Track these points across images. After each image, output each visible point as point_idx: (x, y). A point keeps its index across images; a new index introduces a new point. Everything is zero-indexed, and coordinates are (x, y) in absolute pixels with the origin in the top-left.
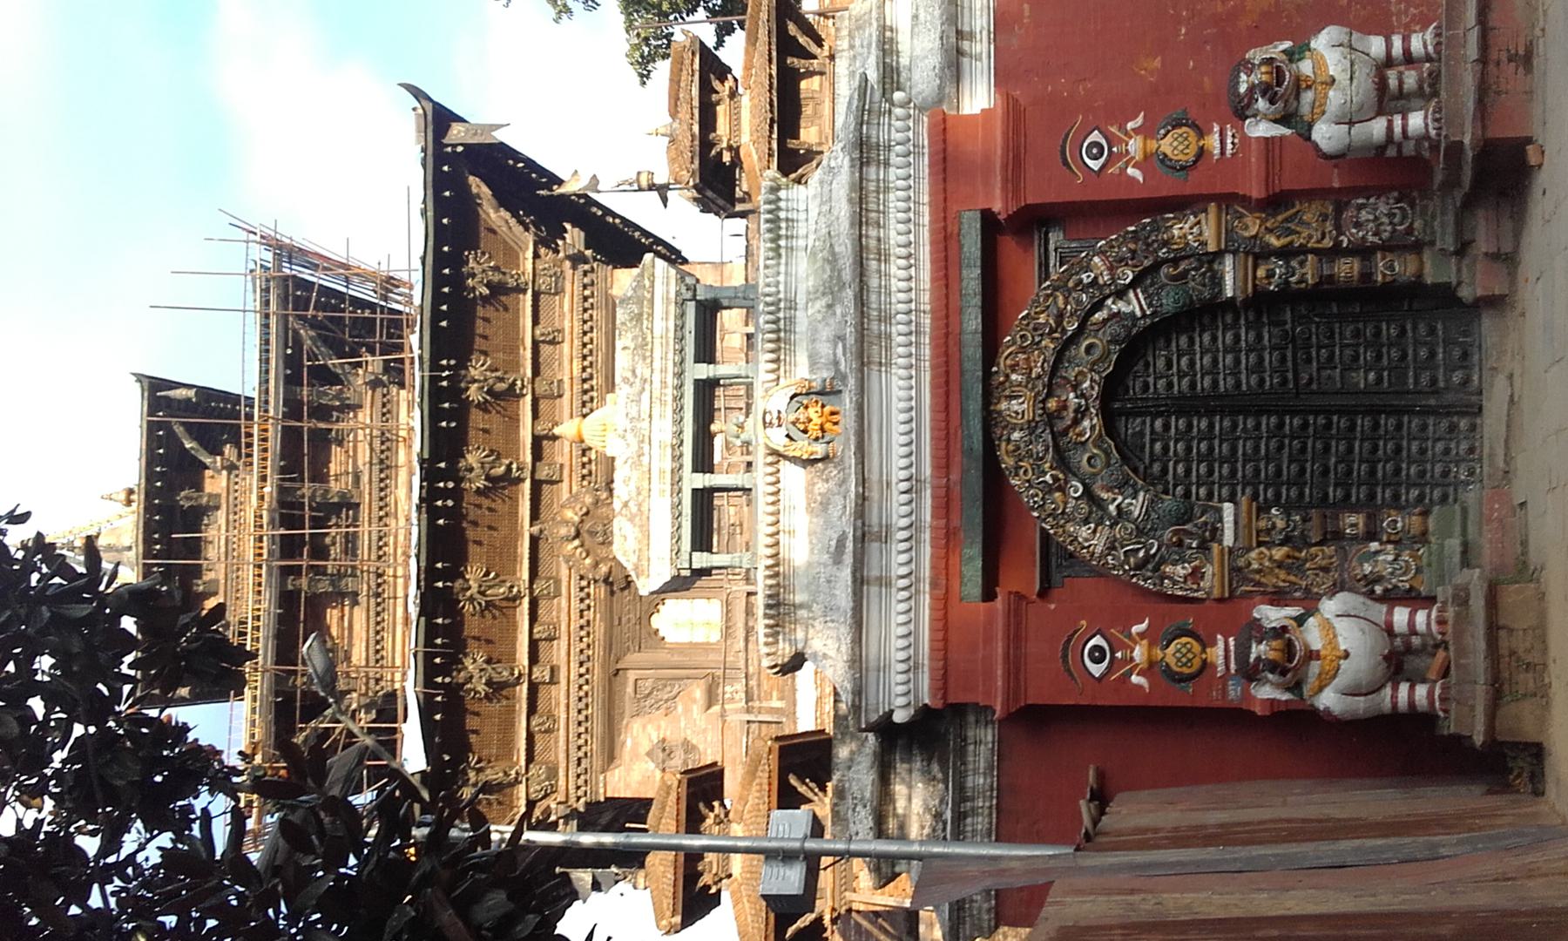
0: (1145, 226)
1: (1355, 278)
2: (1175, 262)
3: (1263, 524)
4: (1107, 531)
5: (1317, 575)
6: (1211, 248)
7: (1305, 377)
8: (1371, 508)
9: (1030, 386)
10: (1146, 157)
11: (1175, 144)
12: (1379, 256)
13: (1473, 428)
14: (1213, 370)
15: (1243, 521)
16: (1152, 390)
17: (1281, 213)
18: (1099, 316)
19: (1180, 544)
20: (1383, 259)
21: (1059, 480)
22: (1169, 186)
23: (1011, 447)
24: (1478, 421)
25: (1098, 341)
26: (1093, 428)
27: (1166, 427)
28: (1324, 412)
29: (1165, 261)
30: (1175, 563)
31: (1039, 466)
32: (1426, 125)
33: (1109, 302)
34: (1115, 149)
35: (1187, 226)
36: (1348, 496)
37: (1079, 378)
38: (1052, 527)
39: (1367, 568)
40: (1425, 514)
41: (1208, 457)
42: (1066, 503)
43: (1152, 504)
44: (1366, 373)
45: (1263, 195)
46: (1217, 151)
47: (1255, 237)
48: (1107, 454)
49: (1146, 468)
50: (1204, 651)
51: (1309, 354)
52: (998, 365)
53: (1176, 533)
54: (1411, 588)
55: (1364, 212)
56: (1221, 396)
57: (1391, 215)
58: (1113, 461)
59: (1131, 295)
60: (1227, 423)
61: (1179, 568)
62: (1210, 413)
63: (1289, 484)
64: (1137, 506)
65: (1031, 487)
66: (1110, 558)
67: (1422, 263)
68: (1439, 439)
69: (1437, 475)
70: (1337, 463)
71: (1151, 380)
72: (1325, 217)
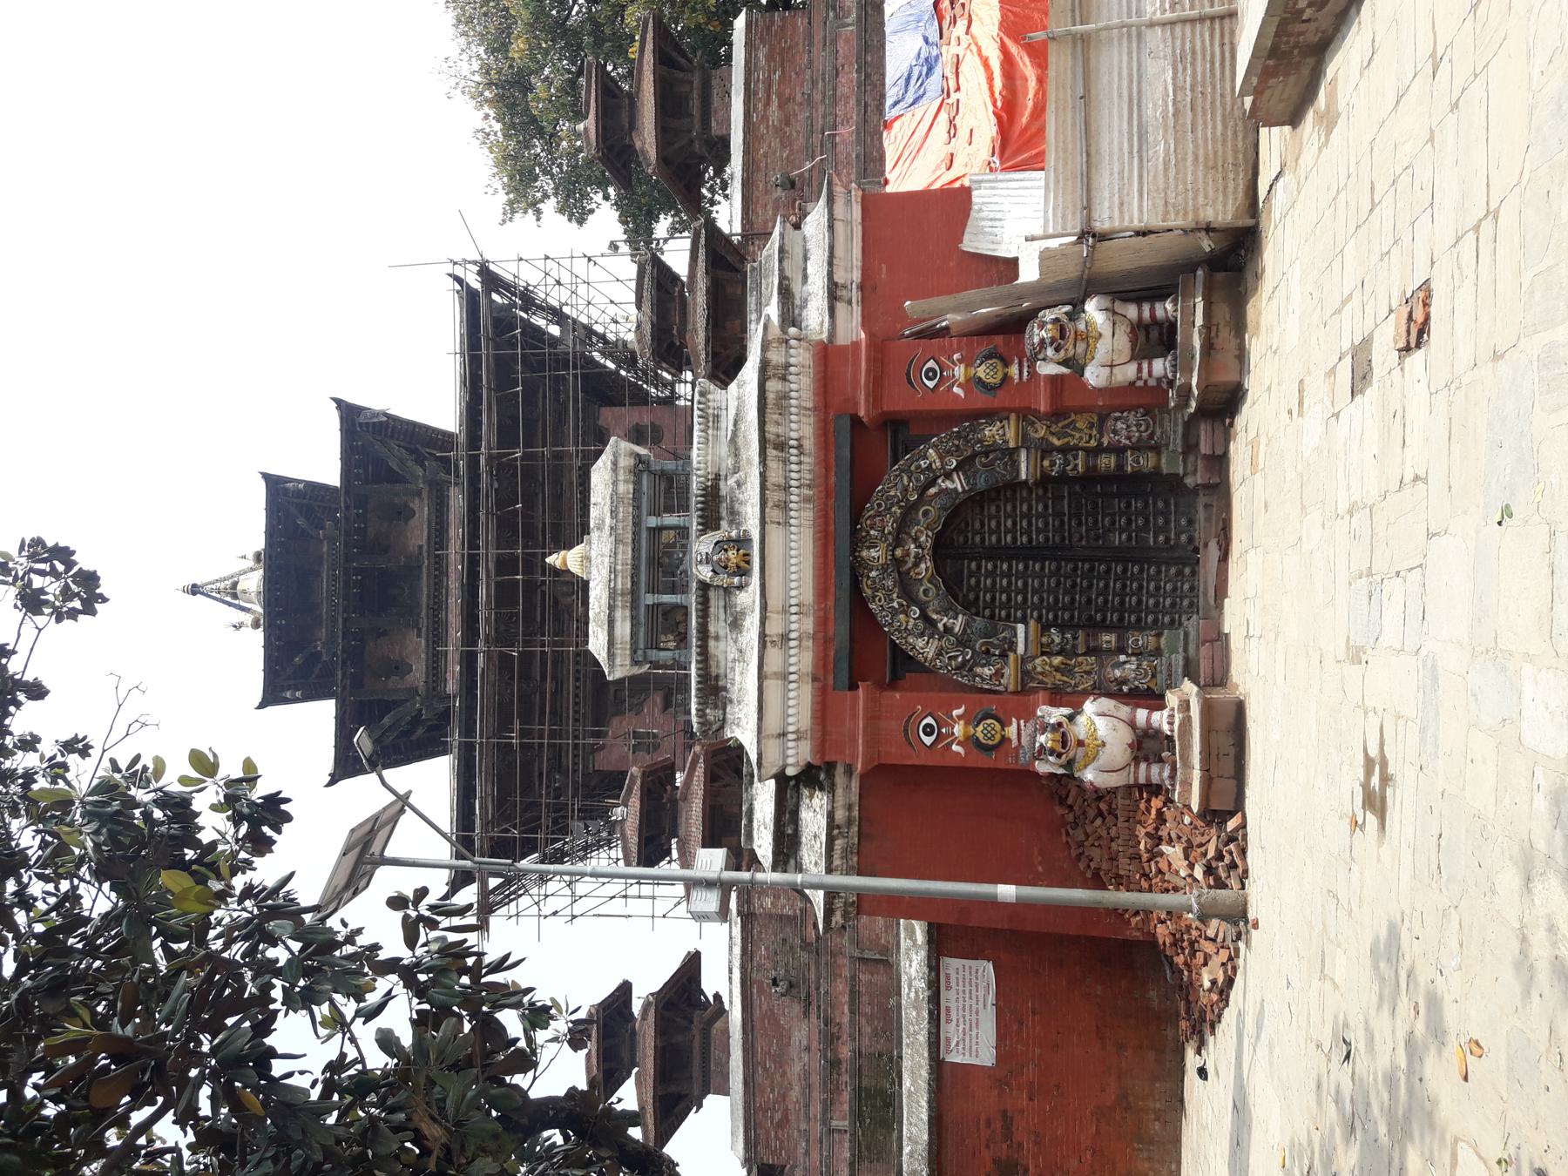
0: (966, 428)
3: (1044, 640)
4: (936, 642)
6: (1012, 445)
7: (1076, 537)
8: (1120, 628)
10: (968, 380)
13: (1194, 573)
14: (1013, 531)
18: (933, 491)
19: (988, 651)
22: (982, 401)
26: (927, 569)
29: (978, 453)
30: (983, 666)
33: (940, 481)
36: (1104, 620)
39: (1118, 673)
40: (1159, 635)
41: (1007, 590)
42: (907, 622)
43: (967, 624)
45: (1048, 409)
46: (1016, 377)
47: (1042, 438)
51: (1080, 520)
57: (1138, 425)
59: (955, 476)
60: (1021, 567)
61: (986, 669)
62: (1009, 559)
63: (1064, 609)
64: (958, 624)
67: (1159, 460)
71: (970, 535)
72: (1091, 426)
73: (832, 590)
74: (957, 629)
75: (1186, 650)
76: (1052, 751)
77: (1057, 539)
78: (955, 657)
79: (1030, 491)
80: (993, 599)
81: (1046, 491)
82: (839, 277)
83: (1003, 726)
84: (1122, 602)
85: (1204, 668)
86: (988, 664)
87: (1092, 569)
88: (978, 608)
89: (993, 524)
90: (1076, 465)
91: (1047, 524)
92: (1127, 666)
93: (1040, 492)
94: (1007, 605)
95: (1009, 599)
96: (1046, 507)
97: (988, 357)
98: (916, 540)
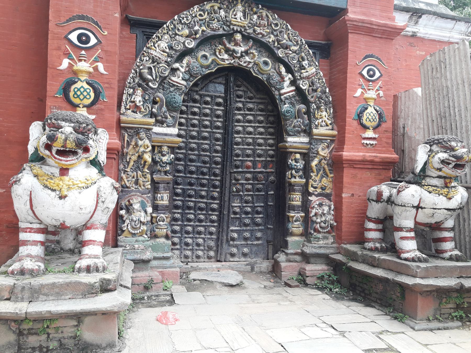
1: (292, 203)
2: (308, 112)
3: (165, 149)
4: (164, 59)
5: (133, 177)
6: (315, 131)
9: (250, 25)
10: (366, 100)
11: (372, 115)
12: (303, 214)
13: (209, 258)
15: (167, 138)
17: (328, 167)
18: (283, 70)
19: (155, 102)
20: (301, 217)
21: (196, 34)
23: (216, 8)
25: (269, 68)
26: (223, 60)
27: (219, 104)
29: (308, 107)
33: (290, 76)
35: (326, 119)
37: (252, 55)
39: (137, 206)
40: (167, 237)
42: (182, 36)
44: (239, 207)
45: (344, 158)
47: (318, 153)
48: (208, 67)
49: (197, 91)
50: (84, 106)
52: (262, 9)
53: (161, 100)
54: (123, 231)
56: (232, 135)
57: (325, 222)
58: (204, 70)
59: (293, 88)
61: (140, 98)
63: (186, 166)
65: (193, 17)
66: (148, 59)
68: (205, 241)
69: (186, 240)
70: (195, 190)
71: (243, 100)
72: (323, 188)
74: (173, 78)
75: (155, 258)
76: (52, 138)
77: (238, 163)
78: (151, 74)
79: (270, 145)
80: (194, 114)
81: (272, 156)
83: (88, 107)
84: (189, 208)
86: (145, 101)
87: (215, 187)
89: (251, 118)
90: (295, 177)
91: (248, 156)
92: (143, 214)
93: (271, 152)
95: (194, 125)
96: (259, 156)
97: (380, 116)
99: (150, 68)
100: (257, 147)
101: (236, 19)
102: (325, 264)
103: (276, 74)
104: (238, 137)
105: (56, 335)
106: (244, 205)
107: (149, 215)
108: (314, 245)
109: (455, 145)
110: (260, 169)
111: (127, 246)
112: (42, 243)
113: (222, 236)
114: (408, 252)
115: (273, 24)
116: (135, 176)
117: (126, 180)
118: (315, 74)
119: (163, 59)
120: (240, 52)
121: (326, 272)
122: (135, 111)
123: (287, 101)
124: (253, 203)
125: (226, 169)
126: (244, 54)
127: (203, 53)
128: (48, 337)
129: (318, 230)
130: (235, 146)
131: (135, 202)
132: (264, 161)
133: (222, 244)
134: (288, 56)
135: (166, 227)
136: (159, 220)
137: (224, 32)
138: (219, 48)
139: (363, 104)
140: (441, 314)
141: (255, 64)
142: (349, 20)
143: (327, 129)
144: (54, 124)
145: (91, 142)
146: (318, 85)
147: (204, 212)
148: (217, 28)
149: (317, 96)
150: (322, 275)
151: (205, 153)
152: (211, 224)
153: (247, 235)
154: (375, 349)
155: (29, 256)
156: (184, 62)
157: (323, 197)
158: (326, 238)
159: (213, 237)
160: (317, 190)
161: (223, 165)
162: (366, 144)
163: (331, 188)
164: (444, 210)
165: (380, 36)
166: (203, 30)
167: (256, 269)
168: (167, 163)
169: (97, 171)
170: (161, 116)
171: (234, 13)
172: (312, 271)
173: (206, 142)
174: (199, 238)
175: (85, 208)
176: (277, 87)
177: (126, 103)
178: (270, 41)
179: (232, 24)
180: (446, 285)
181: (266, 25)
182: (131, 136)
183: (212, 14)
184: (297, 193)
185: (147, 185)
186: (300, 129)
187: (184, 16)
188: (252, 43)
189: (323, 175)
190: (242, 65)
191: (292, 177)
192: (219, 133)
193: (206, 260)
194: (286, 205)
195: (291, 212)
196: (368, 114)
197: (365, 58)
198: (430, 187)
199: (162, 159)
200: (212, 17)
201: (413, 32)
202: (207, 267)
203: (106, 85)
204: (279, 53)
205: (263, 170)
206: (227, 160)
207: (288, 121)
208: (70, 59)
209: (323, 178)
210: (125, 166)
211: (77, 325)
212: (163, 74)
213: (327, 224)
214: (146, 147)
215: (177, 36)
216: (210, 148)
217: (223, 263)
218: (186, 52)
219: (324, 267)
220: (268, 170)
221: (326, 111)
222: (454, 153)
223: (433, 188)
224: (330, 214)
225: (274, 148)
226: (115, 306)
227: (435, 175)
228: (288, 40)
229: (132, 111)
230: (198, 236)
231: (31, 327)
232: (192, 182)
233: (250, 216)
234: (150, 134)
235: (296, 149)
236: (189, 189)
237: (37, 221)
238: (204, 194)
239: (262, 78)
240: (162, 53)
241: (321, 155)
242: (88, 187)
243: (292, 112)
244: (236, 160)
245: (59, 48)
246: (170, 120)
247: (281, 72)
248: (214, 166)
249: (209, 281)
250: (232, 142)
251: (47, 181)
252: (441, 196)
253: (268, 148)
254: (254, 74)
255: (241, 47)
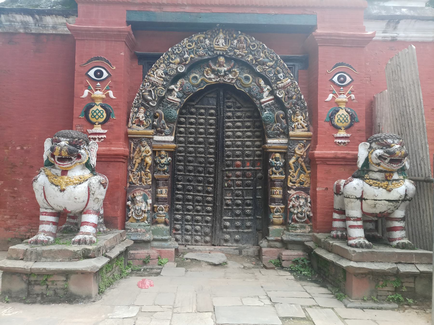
1: (273, 196)
3: (163, 153)
4: (161, 83)
5: (138, 176)
6: (291, 133)
9: (231, 49)
10: (337, 103)
12: (283, 206)
13: (206, 242)
15: (164, 144)
16: (227, 109)
18: (262, 82)
19: (156, 117)
20: (281, 208)
21: (186, 61)
23: (202, 38)
24: (209, 244)
26: (210, 79)
27: (211, 115)
28: (215, 181)
30: (145, 113)
31: (193, 52)
32: (356, 238)
33: (269, 87)
34: (342, 88)
35: (302, 122)
36: (178, 189)
37: (234, 73)
38: (164, 58)
39: (139, 198)
40: (166, 223)
42: (174, 64)
44: (231, 199)
45: (316, 156)
46: (338, 135)
47: (295, 153)
48: (198, 86)
49: (193, 105)
53: (161, 115)
55: (304, 201)
56: (223, 139)
57: (301, 213)
58: (195, 88)
59: (271, 97)
60: (211, 140)
61: (143, 115)
62: (217, 133)
63: (185, 166)
66: (148, 84)
69: (186, 227)
70: (193, 186)
71: (232, 109)
72: (301, 183)
73: (196, 10)
77: (229, 162)
78: (151, 95)
79: (258, 147)
81: (259, 156)
82: (402, 24)
84: (188, 200)
85: (142, 253)
87: (209, 183)
88: (186, 114)
89: (239, 124)
90: (276, 174)
91: (238, 156)
92: (144, 205)
93: (258, 153)
94: (188, 132)
95: (191, 133)
96: (248, 156)
97: (352, 117)
98: (230, 71)
99: (150, 91)
100: (245, 149)
101: (218, 45)
102: (302, 250)
103: (257, 86)
104: (228, 141)
105: (52, 286)
106: (235, 198)
107: (149, 205)
108: (291, 233)
109: (392, 142)
110: (248, 167)
111: (132, 229)
112: (54, 223)
113: (216, 224)
114: (354, 239)
115: (251, 45)
116: (140, 175)
117: (132, 178)
118: (290, 84)
119: (160, 83)
120: (223, 71)
121: (301, 257)
122: (139, 124)
123: (267, 108)
124: (243, 197)
125: (218, 168)
126: (227, 73)
127: (194, 75)
128: (47, 287)
129: (296, 220)
130: (226, 149)
131: (138, 195)
132: (252, 160)
133: (215, 231)
134: (265, 71)
135: (165, 215)
136: (159, 209)
137: (209, 57)
138: (206, 70)
139: (334, 107)
140: (378, 295)
141: (237, 79)
142: (316, 36)
143: (302, 131)
144: (56, 139)
145: (82, 151)
146: (293, 93)
147: (201, 204)
148: (203, 55)
149: (292, 103)
150: (296, 259)
151: (201, 155)
152: (207, 214)
153: (238, 223)
154: (292, 317)
155: (44, 231)
156: (178, 84)
157: (302, 191)
158: (304, 228)
159: (208, 225)
160: (296, 184)
161: (216, 165)
162: (338, 142)
163: (309, 183)
164: (385, 201)
165: (349, 45)
166: (191, 57)
167: (243, 253)
168: (165, 164)
169: (90, 172)
170: (160, 127)
171: (217, 41)
172: (288, 255)
173: (201, 146)
174: (197, 225)
175: (79, 198)
176: (258, 97)
177: (133, 119)
178: (249, 59)
179: (215, 50)
180: (379, 268)
181: (245, 47)
182: (136, 144)
183: (199, 43)
184: (277, 188)
185: (148, 182)
186: (279, 132)
187: (176, 48)
188: (233, 63)
189: (301, 171)
190: (226, 82)
191: (273, 174)
192: (212, 138)
193: (204, 244)
194: (268, 198)
195: (273, 204)
196: (339, 116)
197: (335, 66)
198: (371, 180)
199: (160, 161)
200: (199, 46)
201: (392, 37)
202: (201, 249)
203: (115, 107)
204: (257, 69)
205: (251, 168)
206: (218, 160)
207: (268, 126)
208: (89, 90)
209: (301, 174)
210: (132, 167)
211: (66, 281)
212: (161, 94)
213: (304, 215)
214: (148, 152)
215: (171, 64)
216: (205, 150)
217: (216, 247)
218: (179, 76)
219: (300, 253)
220: (256, 168)
221: (302, 115)
222: (389, 149)
223: (374, 181)
224: (307, 206)
225: (261, 149)
226: (89, 268)
227: (376, 170)
228: (265, 57)
229: (137, 125)
230: (196, 224)
231: (35, 279)
232: (190, 179)
233: (240, 207)
234: (150, 142)
235: (275, 149)
236: (188, 185)
237: (50, 207)
238: (200, 188)
239: (245, 91)
240: (159, 78)
241: (297, 154)
242: (81, 183)
243: (270, 118)
244: (227, 160)
245: (81, 83)
246: (167, 130)
247: (261, 85)
248: (208, 165)
249: (197, 260)
250: (223, 145)
251: (53, 179)
252: (381, 189)
253: (255, 149)
254: (237, 88)
255: (225, 67)
